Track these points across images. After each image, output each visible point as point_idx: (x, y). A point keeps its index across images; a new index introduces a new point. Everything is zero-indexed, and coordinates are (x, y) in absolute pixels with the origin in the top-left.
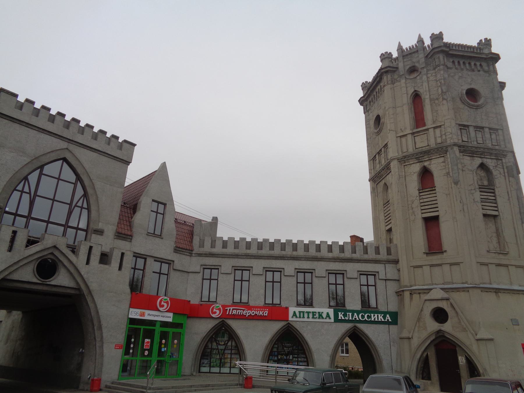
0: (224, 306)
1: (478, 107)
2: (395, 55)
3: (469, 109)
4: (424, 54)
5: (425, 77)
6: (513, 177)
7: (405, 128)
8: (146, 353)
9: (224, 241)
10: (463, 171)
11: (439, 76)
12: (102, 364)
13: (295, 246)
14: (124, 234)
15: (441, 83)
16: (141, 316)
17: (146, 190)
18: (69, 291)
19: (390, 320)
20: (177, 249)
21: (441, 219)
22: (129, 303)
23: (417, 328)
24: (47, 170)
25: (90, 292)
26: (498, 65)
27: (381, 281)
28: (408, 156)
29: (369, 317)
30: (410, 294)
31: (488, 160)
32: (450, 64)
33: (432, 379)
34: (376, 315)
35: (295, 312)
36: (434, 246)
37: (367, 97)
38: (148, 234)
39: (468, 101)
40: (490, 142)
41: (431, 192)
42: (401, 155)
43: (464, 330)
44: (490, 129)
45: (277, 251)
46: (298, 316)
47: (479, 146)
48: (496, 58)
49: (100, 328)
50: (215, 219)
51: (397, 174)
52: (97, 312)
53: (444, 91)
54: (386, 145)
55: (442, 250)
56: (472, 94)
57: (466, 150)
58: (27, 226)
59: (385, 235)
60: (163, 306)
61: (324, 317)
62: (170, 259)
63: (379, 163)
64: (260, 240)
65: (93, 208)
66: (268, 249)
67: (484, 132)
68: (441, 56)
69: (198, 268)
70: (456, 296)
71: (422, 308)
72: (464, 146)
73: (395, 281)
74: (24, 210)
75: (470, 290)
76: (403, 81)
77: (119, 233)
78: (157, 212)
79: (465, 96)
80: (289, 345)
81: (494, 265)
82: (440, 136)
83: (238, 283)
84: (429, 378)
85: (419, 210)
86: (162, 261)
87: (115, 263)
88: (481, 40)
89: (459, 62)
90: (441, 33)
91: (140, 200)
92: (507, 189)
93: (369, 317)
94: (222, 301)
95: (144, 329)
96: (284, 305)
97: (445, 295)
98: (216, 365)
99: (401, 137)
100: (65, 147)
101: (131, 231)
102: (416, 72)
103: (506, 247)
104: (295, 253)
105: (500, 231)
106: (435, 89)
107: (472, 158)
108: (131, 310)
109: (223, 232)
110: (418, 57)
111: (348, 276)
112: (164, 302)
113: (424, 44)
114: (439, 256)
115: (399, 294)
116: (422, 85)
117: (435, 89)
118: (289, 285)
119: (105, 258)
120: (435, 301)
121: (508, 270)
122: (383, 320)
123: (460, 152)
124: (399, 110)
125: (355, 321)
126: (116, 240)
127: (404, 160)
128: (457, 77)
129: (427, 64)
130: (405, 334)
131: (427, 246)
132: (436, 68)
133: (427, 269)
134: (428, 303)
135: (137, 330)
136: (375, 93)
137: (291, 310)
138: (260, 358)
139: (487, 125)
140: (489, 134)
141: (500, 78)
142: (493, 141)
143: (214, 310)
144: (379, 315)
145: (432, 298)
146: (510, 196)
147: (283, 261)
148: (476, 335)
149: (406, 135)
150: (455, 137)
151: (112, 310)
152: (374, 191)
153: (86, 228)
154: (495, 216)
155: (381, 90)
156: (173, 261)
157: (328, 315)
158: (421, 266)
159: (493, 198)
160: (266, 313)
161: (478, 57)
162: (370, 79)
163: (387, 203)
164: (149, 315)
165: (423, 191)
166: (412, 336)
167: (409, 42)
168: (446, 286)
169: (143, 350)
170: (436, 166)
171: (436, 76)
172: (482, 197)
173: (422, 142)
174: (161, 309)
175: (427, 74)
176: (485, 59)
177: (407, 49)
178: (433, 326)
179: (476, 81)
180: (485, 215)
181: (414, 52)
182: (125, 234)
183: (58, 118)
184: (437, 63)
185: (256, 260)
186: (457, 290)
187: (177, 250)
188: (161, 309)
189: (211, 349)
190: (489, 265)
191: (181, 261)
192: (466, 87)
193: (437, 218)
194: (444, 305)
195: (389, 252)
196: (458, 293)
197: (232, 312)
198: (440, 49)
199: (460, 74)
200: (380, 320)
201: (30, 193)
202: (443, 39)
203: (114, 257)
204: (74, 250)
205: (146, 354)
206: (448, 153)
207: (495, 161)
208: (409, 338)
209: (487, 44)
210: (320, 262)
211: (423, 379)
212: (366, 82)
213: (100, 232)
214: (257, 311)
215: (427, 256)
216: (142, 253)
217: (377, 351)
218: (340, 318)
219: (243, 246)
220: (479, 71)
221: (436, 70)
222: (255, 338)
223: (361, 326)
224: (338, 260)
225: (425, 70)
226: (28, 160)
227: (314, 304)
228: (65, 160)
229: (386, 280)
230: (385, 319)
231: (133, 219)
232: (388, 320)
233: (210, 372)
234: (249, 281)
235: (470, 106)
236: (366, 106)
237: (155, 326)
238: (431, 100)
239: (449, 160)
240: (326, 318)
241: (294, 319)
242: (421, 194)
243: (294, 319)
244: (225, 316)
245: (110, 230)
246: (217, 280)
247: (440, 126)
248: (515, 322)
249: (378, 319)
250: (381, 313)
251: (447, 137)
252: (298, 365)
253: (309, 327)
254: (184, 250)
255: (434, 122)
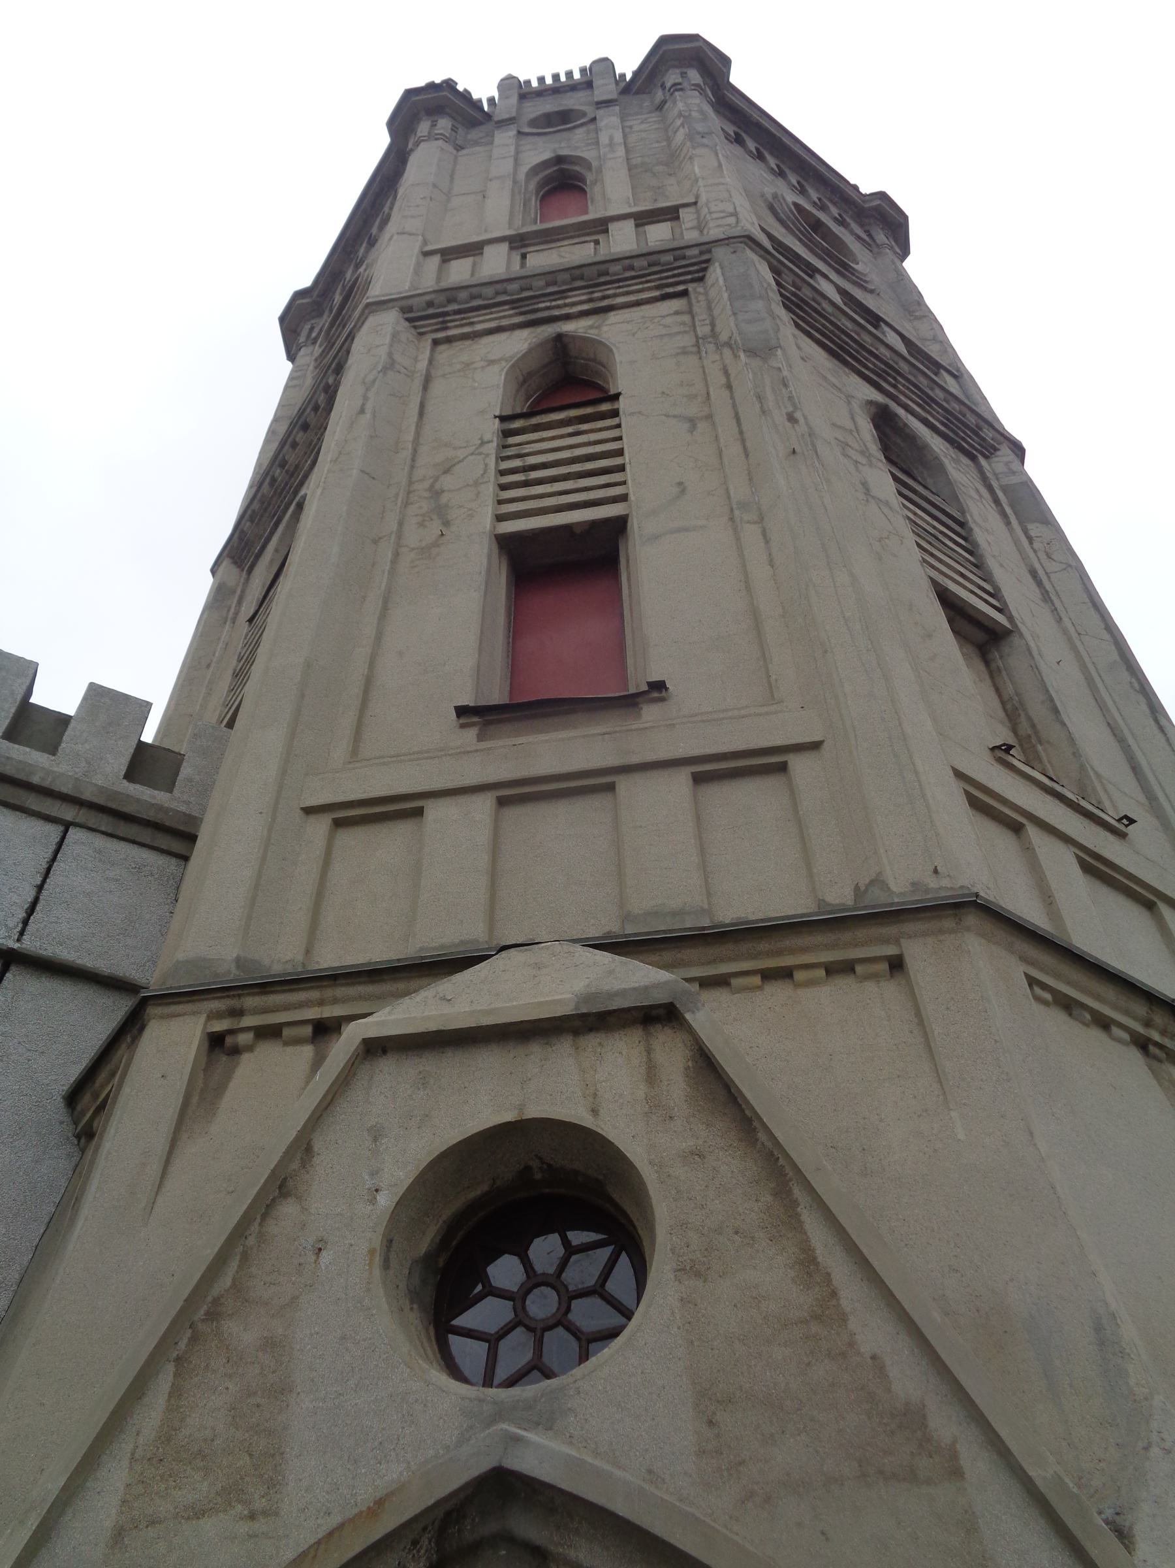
23: (115, 1476)
30: (216, 1041)
70: (740, 1025)
71: (302, 1148)
75: (919, 952)
97: (639, 978)
105: (1037, 710)
120: (489, 1062)
134: (392, 1079)
158: (402, 809)
196: (778, 992)
215: (481, 737)
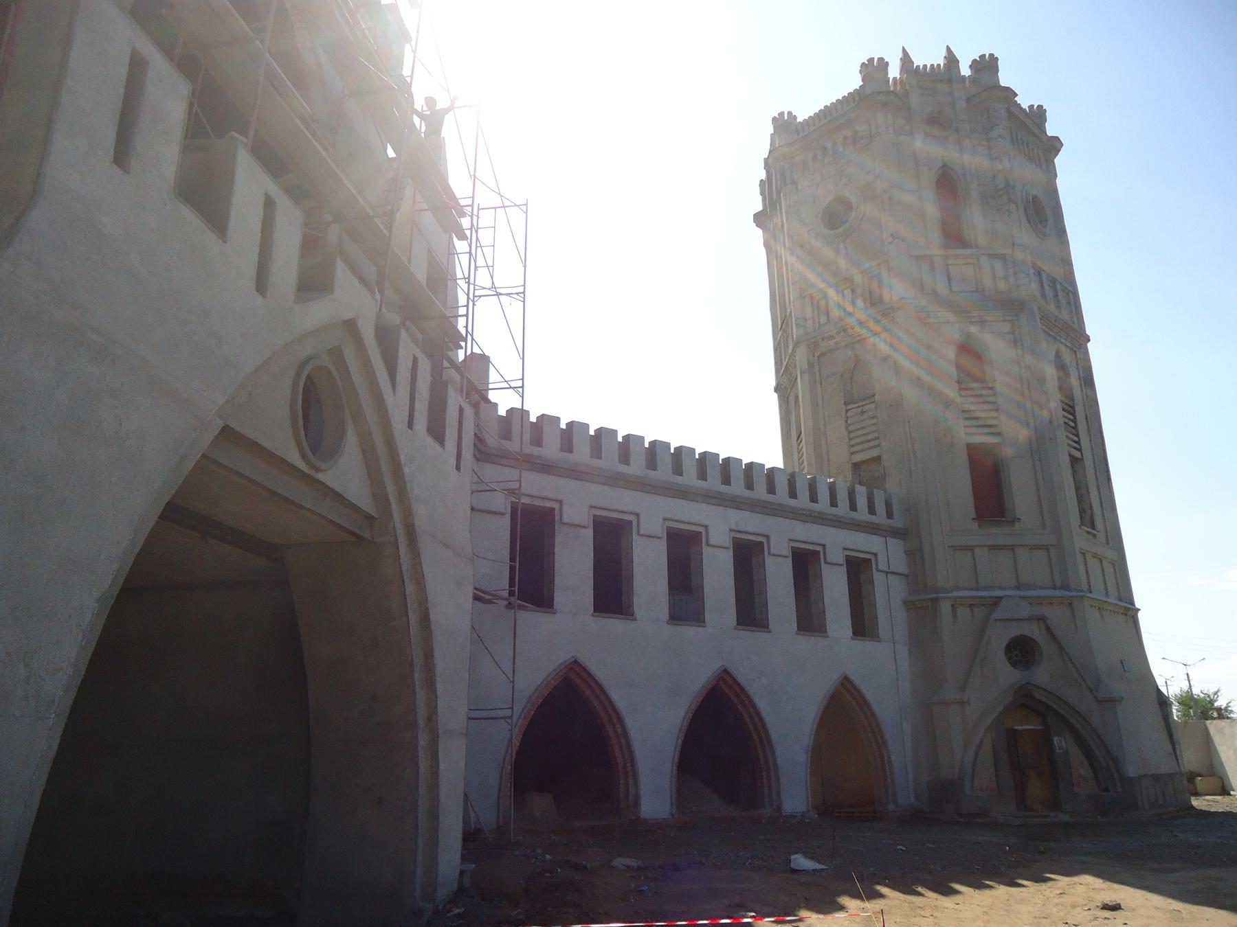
158: (970, 549)
167: (928, 56)
178: (1008, 676)
194: (1033, 631)
208: (962, 703)
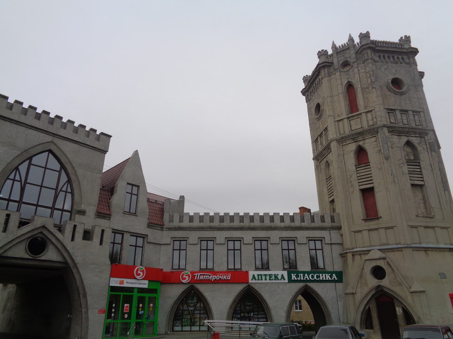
0: (192, 273)
1: (402, 94)
2: (330, 52)
3: (394, 95)
4: (355, 50)
5: (356, 70)
6: (435, 152)
7: (342, 114)
8: (126, 316)
9: (190, 216)
10: (392, 148)
11: (368, 69)
12: (87, 328)
13: (252, 218)
14: (104, 213)
15: (370, 74)
16: (120, 284)
17: (121, 175)
18: (57, 265)
19: (336, 279)
20: (150, 225)
21: (376, 190)
22: (110, 272)
23: (359, 284)
24: (35, 160)
25: (75, 265)
26: (417, 58)
27: (327, 245)
28: (346, 137)
29: (318, 277)
30: (353, 255)
31: (414, 139)
32: (377, 58)
33: (374, 328)
34: (324, 275)
35: (254, 275)
36: (371, 213)
37: (308, 89)
38: (125, 213)
39: (394, 88)
40: (414, 123)
41: (366, 167)
42: (339, 137)
43: (400, 284)
44: (413, 111)
45: (237, 223)
46: (257, 278)
47: (404, 126)
48: (415, 52)
49: (85, 295)
50: (182, 198)
51: (336, 152)
52: (82, 282)
53: (373, 80)
54: (326, 129)
55: (378, 216)
56: (396, 83)
57: (394, 130)
58: (18, 210)
59: (329, 205)
60: (139, 274)
61: (280, 278)
62: (144, 233)
63: (321, 144)
64: (222, 214)
65: (76, 192)
66: (229, 221)
67: (408, 115)
68: (369, 51)
69: (168, 241)
70: (390, 255)
71: (363, 267)
72: (392, 127)
73: (338, 245)
74: (16, 196)
75: (403, 250)
76: (338, 74)
77: (99, 213)
78: (132, 194)
79: (391, 85)
80: (250, 304)
81: (423, 228)
82: (371, 119)
83: (204, 252)
84: (371, 327)
85: (357, 183)
86: (136, 235)
87: (96, 239)
88: (402, 38)
89: (384, 56)
90: (368, 32)
91: (116, 184)
92: (430, 161)
93: (318, 277)
94: (190, 268)
95: (123, 295)
96: (244, 269)
97: (383, 255)
98: (187, 324)
99: (338, 121)
100: (50, 140)
101: (110, 210)
102: (348, 66)
103: (432, 212)
104: (252, 224)
105: (426, 198)
106: (366, 79)
107: (399, 137)
108: (112, 279)
109: (190, 209)
110: (350, 53)
111: (299, 242)
112: (140, 271)
113: (354, 42)
114: (376, 222)
115: (343, 256)
116: (354, 77)
117: (366, 79)
118: (248, 251)
119: (87, 235)
120: (374, 261)
121: (435, 231)
122: (330, 279)
123: (389, 132)
124: (335, 98)
125: (306, 281)
126: (96, 219)
127: (342, 141)
128: (383, 69)
129: (357, 59)
130: (350, 290)
131: (365, 213)
132: (365, 61)
133: (365, 233)
134: (367, 261)
135: (117, 297)
136: (315, 85)
137: (251, 273)
138: (225, 316)
139: (410, 109)
140: (413, 116)
141: (420, 69)
142: (417, 122)
143: (184, 276)
144: (327, 275)
145: (371, 258)
146: (433, 168)
147: (241, 231)
148: (410, 288)
149: (342, 119)
150: (384, 119)
151: (95, 280)
152: (317, 168)
153: (70, 210)
154: (421, 186)
155: (320, 82)
156: (147, 235)
157: (283, 277)
158: (360, 231)
159: (419, 170)
160: (229, 277)
161: (400, 52)
162: (310, 73)
163: (329, 178)
164: (127, 283)
165: (360, 166)
166: (356, 292)
167: (341, 41)
168: (382, 247)
169: (123, 314)
170: (369, 145)
171: (365, 69)
172: (410, 170)
173: (356, 125)
174: (138, 277)
175: (358, 67)
176: (406, 53)
177: (340, 47)
178: (373, 282)
179: (400, 72)
180: (413, 185)
181: (346, 49)
182: (104, 214)
183: (44, 116)
184: (366, 58)
185: (219, 231)
186: (392, 250)
187: (150, 225)
188: (138, 277)
189: (183, 310)
190: (418, 227)
191: (154, 235)
192: (391, 77)
193: (372, 189)
194: (381, 264)
195: (333, 220)
196: (393, 253)
197: (200, 278)
198: (368, 46)
199: (386, 67)
200: (327, 279)
201: (21, 181)
202: (370, 37)
203: (95, 234)
204: (60, 229)
205: (126, 317)
206: (379, 133)
207: (419, 138)
208: (353, 294)
209: (407, 41)
210: (273, 232)
211: (366, 328)
212: (307, 76)
213: (82, 213)
214: (222, 275)
216: (120, 229)
217: (326, 306)
218: (293, 279)
219: (207, 219)
220: (401, 63)
221: (366, 63)
222: (220, 299)
223: (311, 285)
224: (289, 229)
225: (356, 63)
226: (19, 153)
227: (270, 267)
228: (50, 151)
229: (331, 244)
230: (331, 278)
231: (111, 200)
232: (334, 279)
233: (182, 331)
234: (213, 250)
235: (396, 93)
236: (308, 96)
237: (133, 292)
238: (362, 89)
239: (380, 140)
240: (281, 279)
241: (254, 281)
242: (358, 169)
243: (254, 281)
244: (194, 281)
245: (91, 211)
246: (186, 250)
247: (371, 111)
248: (443, 276)
249: (326, 278)
250: (328, 273)
251: (378, 120)
252: (258, 321)
253: (267, 288)
254: (156, 226)
255: (366, 108)
